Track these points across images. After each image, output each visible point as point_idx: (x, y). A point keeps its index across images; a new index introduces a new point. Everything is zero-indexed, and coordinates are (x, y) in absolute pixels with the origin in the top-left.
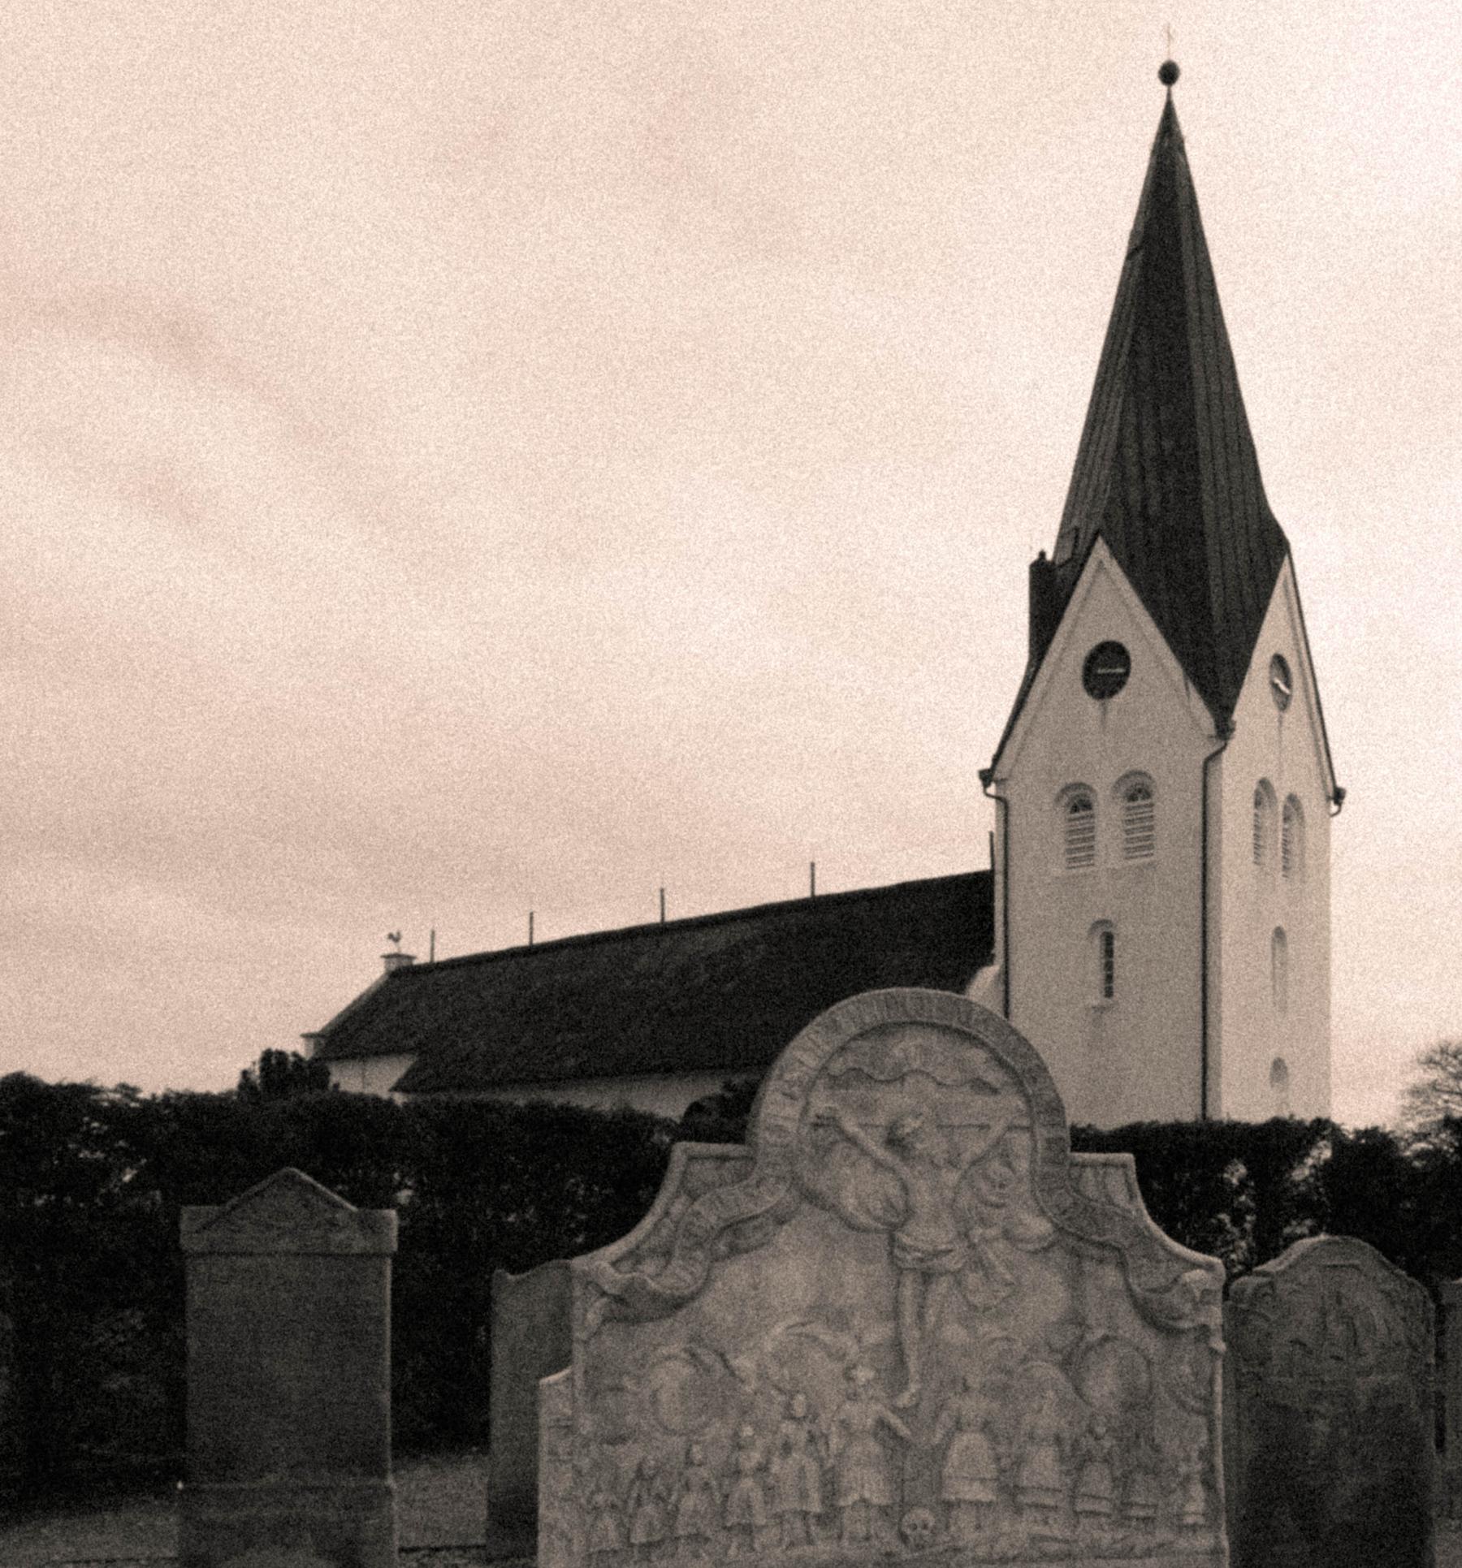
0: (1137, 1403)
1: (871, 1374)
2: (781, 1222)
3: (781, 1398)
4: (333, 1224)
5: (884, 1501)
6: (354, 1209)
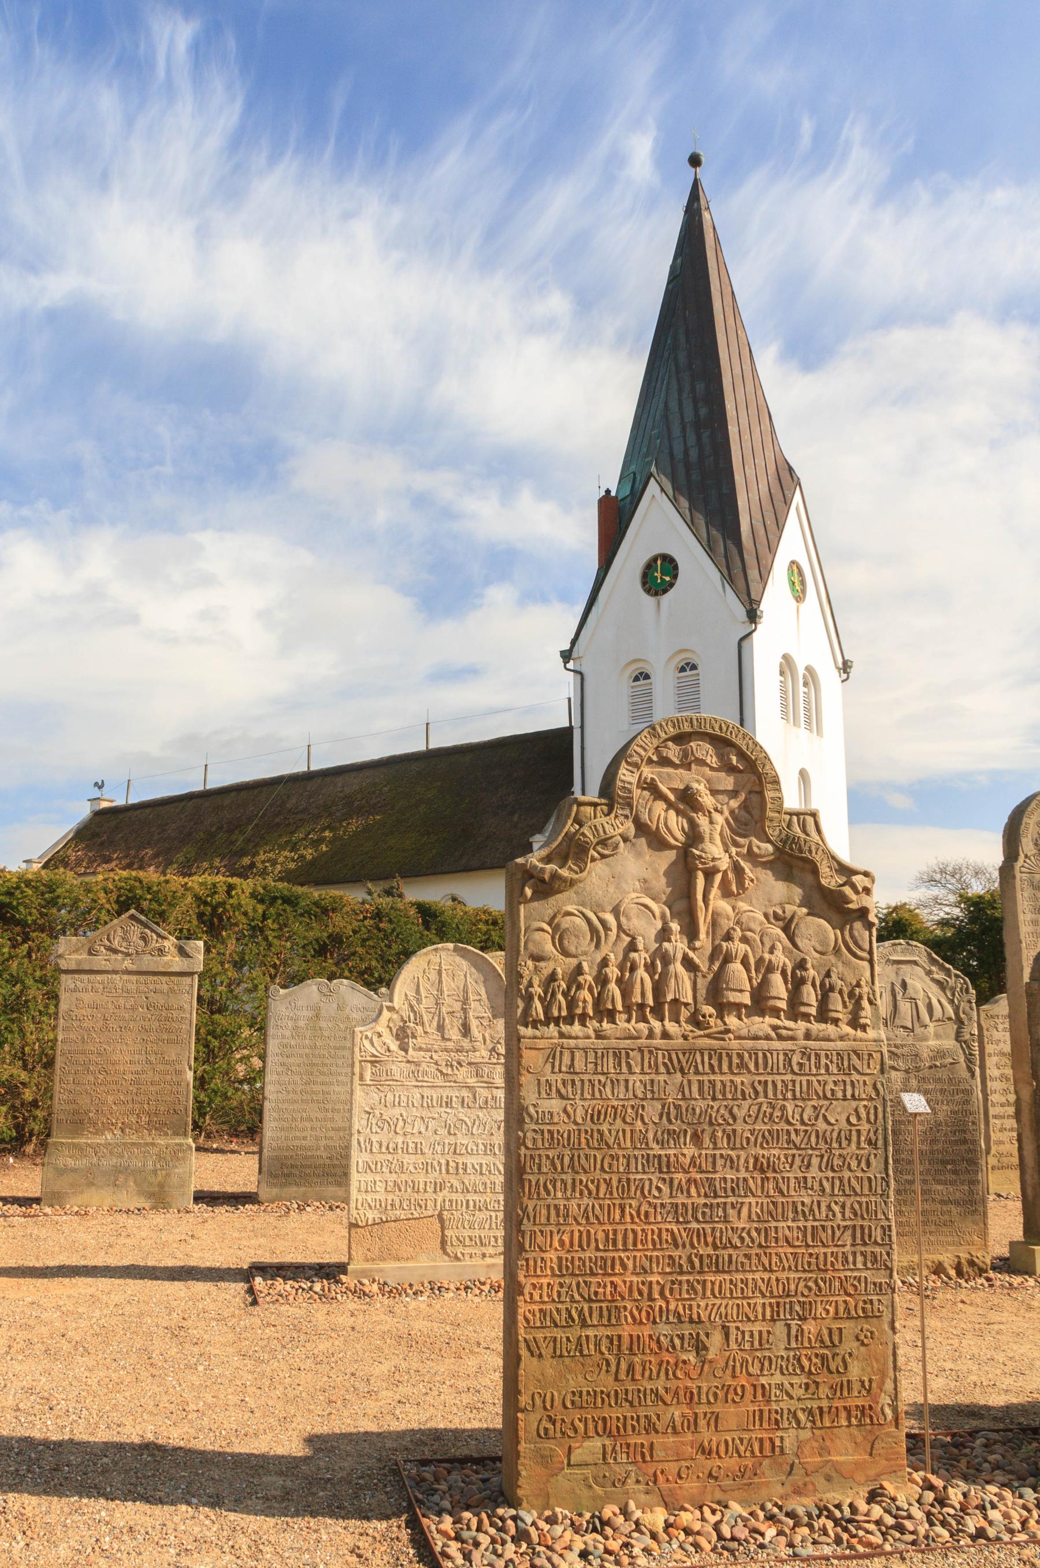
1: (679, 928)
3: (628, 939)
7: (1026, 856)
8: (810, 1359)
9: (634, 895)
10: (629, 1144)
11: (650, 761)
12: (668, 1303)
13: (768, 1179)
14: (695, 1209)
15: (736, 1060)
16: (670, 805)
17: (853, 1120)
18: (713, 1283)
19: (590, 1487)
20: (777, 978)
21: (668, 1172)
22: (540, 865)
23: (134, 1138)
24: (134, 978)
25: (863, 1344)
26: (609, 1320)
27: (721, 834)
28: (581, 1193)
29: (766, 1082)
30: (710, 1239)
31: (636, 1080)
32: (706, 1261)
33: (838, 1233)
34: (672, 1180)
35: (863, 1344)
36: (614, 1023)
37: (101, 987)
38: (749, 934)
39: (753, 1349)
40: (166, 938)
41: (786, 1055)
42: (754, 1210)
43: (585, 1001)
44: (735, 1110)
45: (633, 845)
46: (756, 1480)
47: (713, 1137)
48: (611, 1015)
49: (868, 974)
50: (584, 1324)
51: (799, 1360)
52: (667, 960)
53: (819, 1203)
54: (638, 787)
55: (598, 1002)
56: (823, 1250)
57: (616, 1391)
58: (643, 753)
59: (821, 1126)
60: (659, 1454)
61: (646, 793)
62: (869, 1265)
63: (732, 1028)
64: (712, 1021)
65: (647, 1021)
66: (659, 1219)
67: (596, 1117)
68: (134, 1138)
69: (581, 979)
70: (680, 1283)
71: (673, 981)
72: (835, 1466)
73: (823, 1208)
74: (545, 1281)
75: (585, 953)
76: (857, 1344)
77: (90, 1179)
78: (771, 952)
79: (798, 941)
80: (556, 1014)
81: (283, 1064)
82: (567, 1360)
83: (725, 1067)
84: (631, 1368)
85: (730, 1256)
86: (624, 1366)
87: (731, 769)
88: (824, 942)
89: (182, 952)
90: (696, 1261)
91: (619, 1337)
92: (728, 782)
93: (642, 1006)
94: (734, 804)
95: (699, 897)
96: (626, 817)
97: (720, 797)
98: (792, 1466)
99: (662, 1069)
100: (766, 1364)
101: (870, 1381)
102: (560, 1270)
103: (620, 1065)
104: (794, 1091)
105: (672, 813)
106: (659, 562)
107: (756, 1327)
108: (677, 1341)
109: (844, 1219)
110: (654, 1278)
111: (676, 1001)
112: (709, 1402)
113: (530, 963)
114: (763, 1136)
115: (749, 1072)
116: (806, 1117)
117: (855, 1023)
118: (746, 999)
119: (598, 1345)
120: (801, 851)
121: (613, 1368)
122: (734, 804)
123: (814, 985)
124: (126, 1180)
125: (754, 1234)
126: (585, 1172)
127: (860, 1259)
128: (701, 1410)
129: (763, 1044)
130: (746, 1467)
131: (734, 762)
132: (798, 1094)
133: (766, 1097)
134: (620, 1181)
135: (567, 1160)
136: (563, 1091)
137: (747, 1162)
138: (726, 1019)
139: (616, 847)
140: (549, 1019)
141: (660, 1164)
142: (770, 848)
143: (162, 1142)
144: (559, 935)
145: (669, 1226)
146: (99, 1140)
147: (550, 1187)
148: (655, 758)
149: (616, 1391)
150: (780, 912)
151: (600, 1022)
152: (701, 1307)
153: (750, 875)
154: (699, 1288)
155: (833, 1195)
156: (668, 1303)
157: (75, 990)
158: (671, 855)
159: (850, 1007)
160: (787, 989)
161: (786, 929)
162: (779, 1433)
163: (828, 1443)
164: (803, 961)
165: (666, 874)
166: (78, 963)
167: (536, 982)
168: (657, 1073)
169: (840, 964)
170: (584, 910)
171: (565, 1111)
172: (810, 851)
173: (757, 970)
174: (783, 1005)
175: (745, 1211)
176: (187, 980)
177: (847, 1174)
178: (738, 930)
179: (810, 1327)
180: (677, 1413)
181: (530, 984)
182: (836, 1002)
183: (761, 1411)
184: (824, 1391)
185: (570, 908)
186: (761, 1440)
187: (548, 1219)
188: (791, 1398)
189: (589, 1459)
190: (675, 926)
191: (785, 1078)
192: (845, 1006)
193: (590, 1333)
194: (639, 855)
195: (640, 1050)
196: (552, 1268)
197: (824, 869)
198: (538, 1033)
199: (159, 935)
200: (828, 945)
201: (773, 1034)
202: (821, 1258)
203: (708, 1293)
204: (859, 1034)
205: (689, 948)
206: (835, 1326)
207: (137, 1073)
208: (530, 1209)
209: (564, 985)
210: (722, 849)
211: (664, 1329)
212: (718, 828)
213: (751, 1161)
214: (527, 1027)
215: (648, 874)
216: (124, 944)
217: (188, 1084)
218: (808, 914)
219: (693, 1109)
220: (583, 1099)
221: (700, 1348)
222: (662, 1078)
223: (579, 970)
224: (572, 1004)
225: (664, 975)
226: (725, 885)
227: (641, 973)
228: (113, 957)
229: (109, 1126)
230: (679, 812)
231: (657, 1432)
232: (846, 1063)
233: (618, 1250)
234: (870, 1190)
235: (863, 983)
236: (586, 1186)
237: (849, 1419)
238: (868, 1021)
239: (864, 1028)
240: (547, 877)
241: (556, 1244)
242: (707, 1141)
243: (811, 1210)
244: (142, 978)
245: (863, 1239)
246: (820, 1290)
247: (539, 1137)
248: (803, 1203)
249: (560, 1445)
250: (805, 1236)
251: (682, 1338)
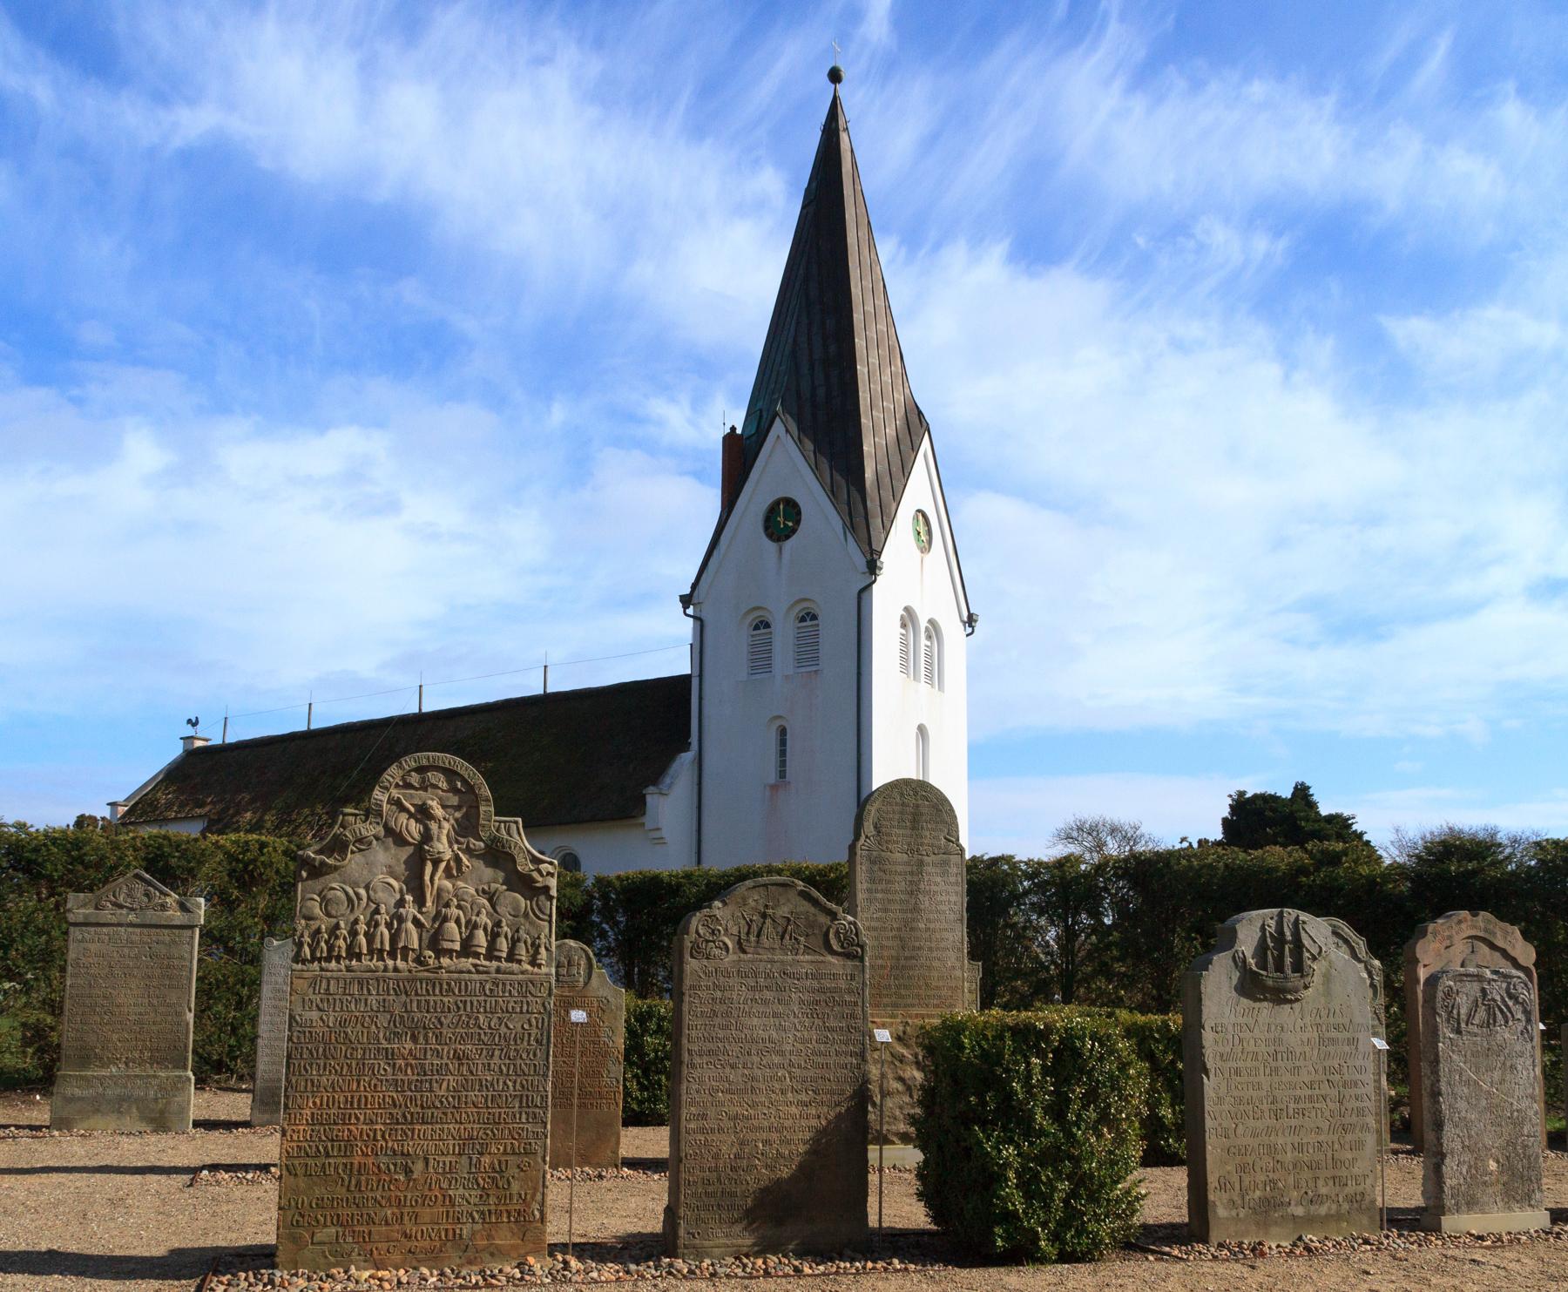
3: (374, 906)
7: (867, 837)
8: (484, 1180)
9: (381, 876)
10: (365, 1040)
11: (397, 786)
12: (387, 1142)
13: (463, 1064)
14: (410, 1083)
15: (445, 986)
16: (411, 815)
17: (526, 1026)
18: (419, 1130)
19: (326, 1257)
20: (480, 934)
21: (393, 1059)
22: (313, 855)
23: (138, 1071)
24: (138, 930)
25: (522, 1170)
26: (345, 1152)
27: (448, 836)
28: (330, 1071)
29: (466, 1001)
30: (419, 1103)
31: (373, 1000)
32: (416, 1116)
33: (510, 1100)
34: (394, 1064)
35: (522, 1170)
36: (361, 961)
37: (107, 938)
38: (462, 903)
39: (444, 1173)
40: (168, 895)
41: (481, 983)
42: (451, 1083)
43: (339, 947)
44: (443, 1019)
45: (383, 842)
46: (442, 1255)
47: (426, 1037)
48: (359, 957)
49: (547, 930)
50: (328, 1155)
51: (476, 1180)
52: (401, 920)
53: (498, 1080)
54: (388, 803)
55: (350, 948)
56: (498, 1110)
57: (347, 1198)
58: (391, 780)
59: (503, 1030)
60: (375, 1237)
61: (394, 807)
62: (531, 1120)
63: (444, 965)
64: (431, 961)
65: (384, 961)
66: (384, 1089)
67: (343, 1023)
68: (138, 1071)
69: (338, 932)
70: (396, 1130)
71: (404, 934)
72: (497, 1247)
73: (501, 1083)
74: (302, 1128)
75: (343, 915)
76: (517, 1170)
77: (97, 1106)
78: (478, 915)
79: (498, 908)
80: (319, 955)
81: (275, 1007)
82: (315, 1179)
83: (437, 992)
84: (358, 1184)
85: (432, 1113)
86: (353, 1182)
87: (455, 790)
88: (516, 908)
89: (183, 907)
90: (409, 1116)
91: (352, 1164)
92: (454, 800)
93: (381, 951)
94: (458, 815)
95: (427, 878)
96: (378, 823)
97: (449, 810)
98: (467, 1246)
99: (392, 992)
100: (453, 1182)
101: (526, 1194)
102: (312, 1120)
103: (362, 989)
104: (485, 1007)
105: (412, 821)
107: (447, 1160)
108: (392, 1167)
109: (515, 1091)
110: (378, 1127)
111: (405, 949)
112: (412, 1206)
113: (303, 922)
114: (461, 1036)
115: (454, 994)
116: (492, 1024)
117: (533, 963)
118: (457, 946)
119: (336, 1168)
120: (503, 846)
121: (346, 1183)
122: (458, 815)
123: (506, 937)
124: (130, 1107)
125: (451, 1099)
126: (333, 1058)
127: (524, 1116)
128: (405, 1211)
130: (435, 1246)
131: (459, 786)
132: (488, 1010)
133: (465, 1010)
134: (357, 1064)
135: (321, 1050)
136: (321, 1005)
137: (448, 1052)
138: (442, 960)
139: (370, 843)
140: (313, 959)
141: (387, 1054)
142: (482, 845)
143: (163, 1075)
144: (326, 902)
145: (391, 1094)
147: (308, 1068)
148: (401, 783)
149: (347, 1198)
150: (486, 888)
151: (351, 960)
152: (409, 1147)
153: (467, 863)
154: (410, 1133)
155: (508, 1075)
156: (387, 1142)
157: (83, 940)
158: (410, 849)
159: (531, 952)
160: (487, 940)
161: (490, 900)
162: (459, 1226)
163: (493, 1232)
164: (500, 921)
165: (405, 862)
166: (86, 916)
167: (306, 934)
168: (388, 995)
169: (527, 925)
170: (344, 886)
171: (321, 1019)
172: (510, 848)
173: (466, 927)
174: (483, 951)
175: (445, 1085)
176: (188, 933)
177: (519, 1062)
178: (455, 900)
179: (486, 1160)
180: (389, 1212)
181: (302, 936)
182: (522, 951)
183: (448, 1212)
184: (492, 1200)
185: (334, 885)
186: (447, 1230)
187: (306, 1088)
188: (469, 1203)
189: (326, 1240)
190: (409, 898)
191: (480, 998)
192: (527, 951)
193: (332, 1161)
194: (387, 849)
195: (377, 980)
196: (307, 1120)
197: (520, 859)
198: (305, 968)
199: (161, 892)
200: (519, 911)
201: (473, 970)
202: (497, 1115)
203: (416, 1137)
204: (536, 970)
205: (419, 912)
206: (503, 1159)
207: (141, 1014)
208: (294, 1081)
209: (326, 936)
210: (447, 845)
211: (385, 1160)
212: (445, 832)
213: (452, 1052)
214: (298, 963)
215: (393, 862)
216: (129, 900)
217: (188, 1024)
218: (507, 890)
219: (413, 1019)
220: (334, 1011)
221: (408, 1171)
222: (391, 998)
223: (337, 926)
224: (331, 948)
225: (399, 929)
226: (448, 870)
227: (383, 929)
228: (119, 911)
229: (113, 1061)
230: (417, 821)
231: (374, 1223)
232: (524, 989)
233: (354, 1109)
234: (535, 1071)
235: (542, 936)
236: (334, 1067)
237: (509, 1217)
238: (544, 962)
239: (539, 966)
240: (317, 864)
241: (311, 1104)
242: (421, 1040)
243: (492, 1084)
244: (145, 930)
245: (527, 1103)
246: (494, 1135)
247: (302, 1036)
248: (486, 1080)
249: (307, 1231)
250: (486, 1101)
251: (395, 1165)
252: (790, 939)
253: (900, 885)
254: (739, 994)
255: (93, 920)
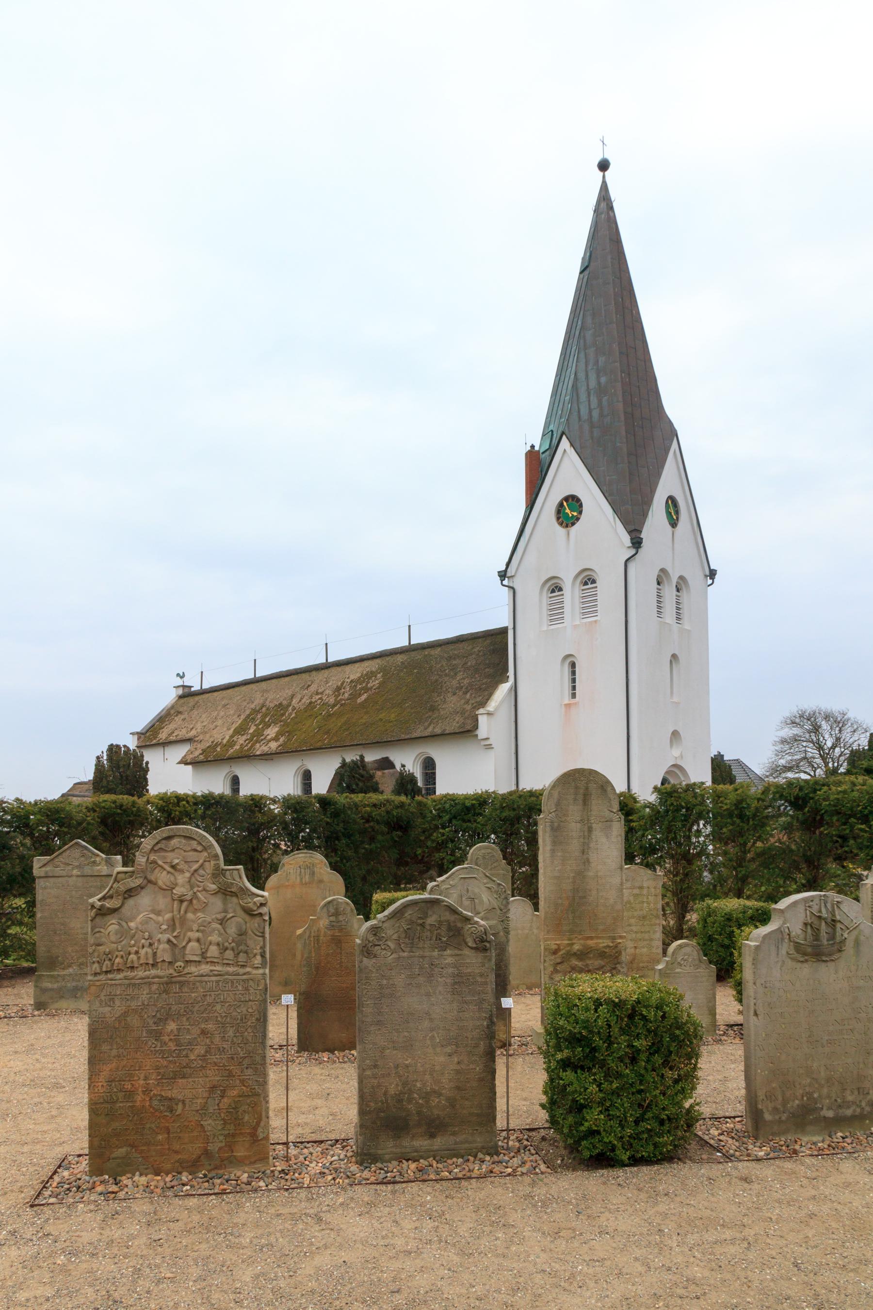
0: (242, 933)
2: (142, 888)
4: (94, 862)
5: (170, 960)
6: (104, 856)
67: (125, 1014)
106: (565, 504)
129: (206, 979)
146: (66, 972)
157: (45, 888)
166: (46, 872)
170: (121, 922)
222: (156, 996)
229: (69, 966)
252: (436, 940)
253: (574, 846)
254: (400, 980)
255: (51, 875)
